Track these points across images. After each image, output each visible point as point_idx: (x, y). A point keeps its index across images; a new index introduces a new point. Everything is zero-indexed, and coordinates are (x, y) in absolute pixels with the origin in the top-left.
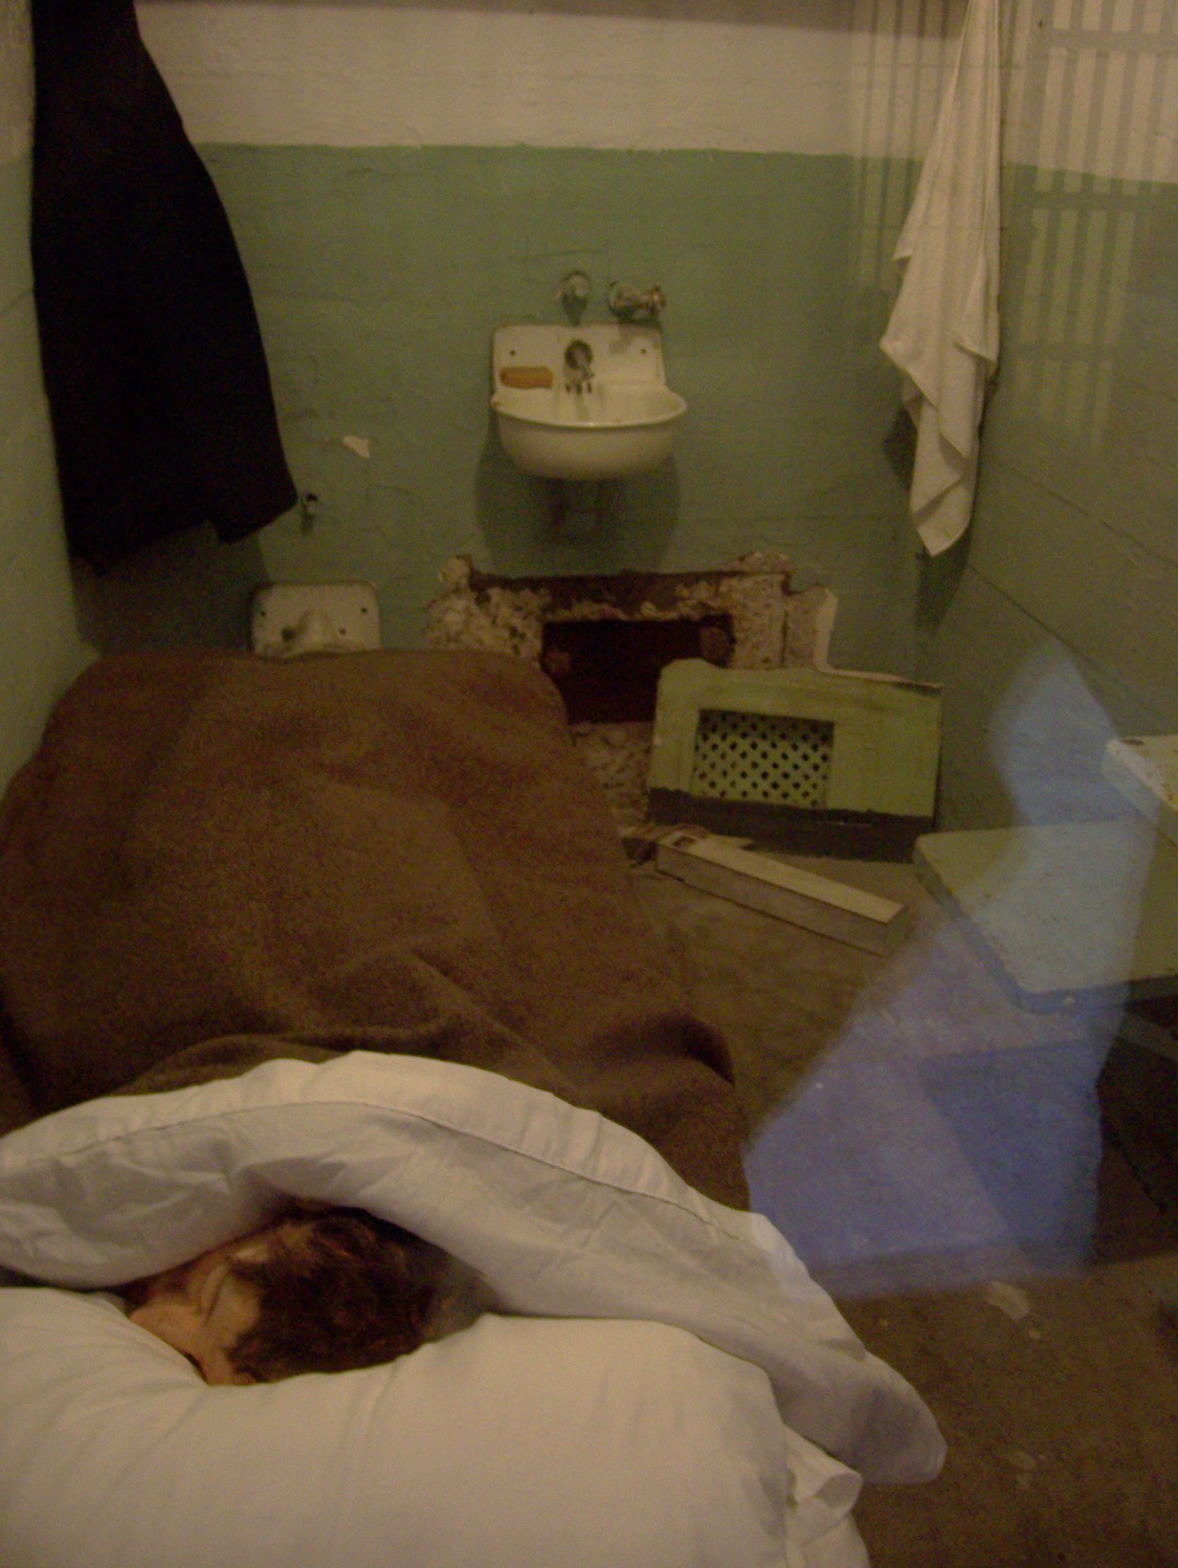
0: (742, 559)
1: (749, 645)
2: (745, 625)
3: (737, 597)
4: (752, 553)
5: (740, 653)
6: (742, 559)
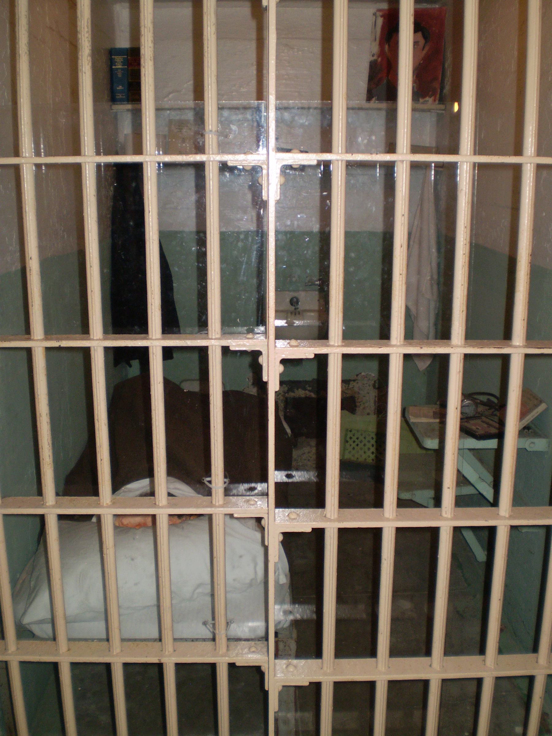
0: (357, 375)
1: (361, 407)
2: (359, 400)
3: (356, 389)
4: (361, 373)
5: (359, 410)
6: (357, 375)
